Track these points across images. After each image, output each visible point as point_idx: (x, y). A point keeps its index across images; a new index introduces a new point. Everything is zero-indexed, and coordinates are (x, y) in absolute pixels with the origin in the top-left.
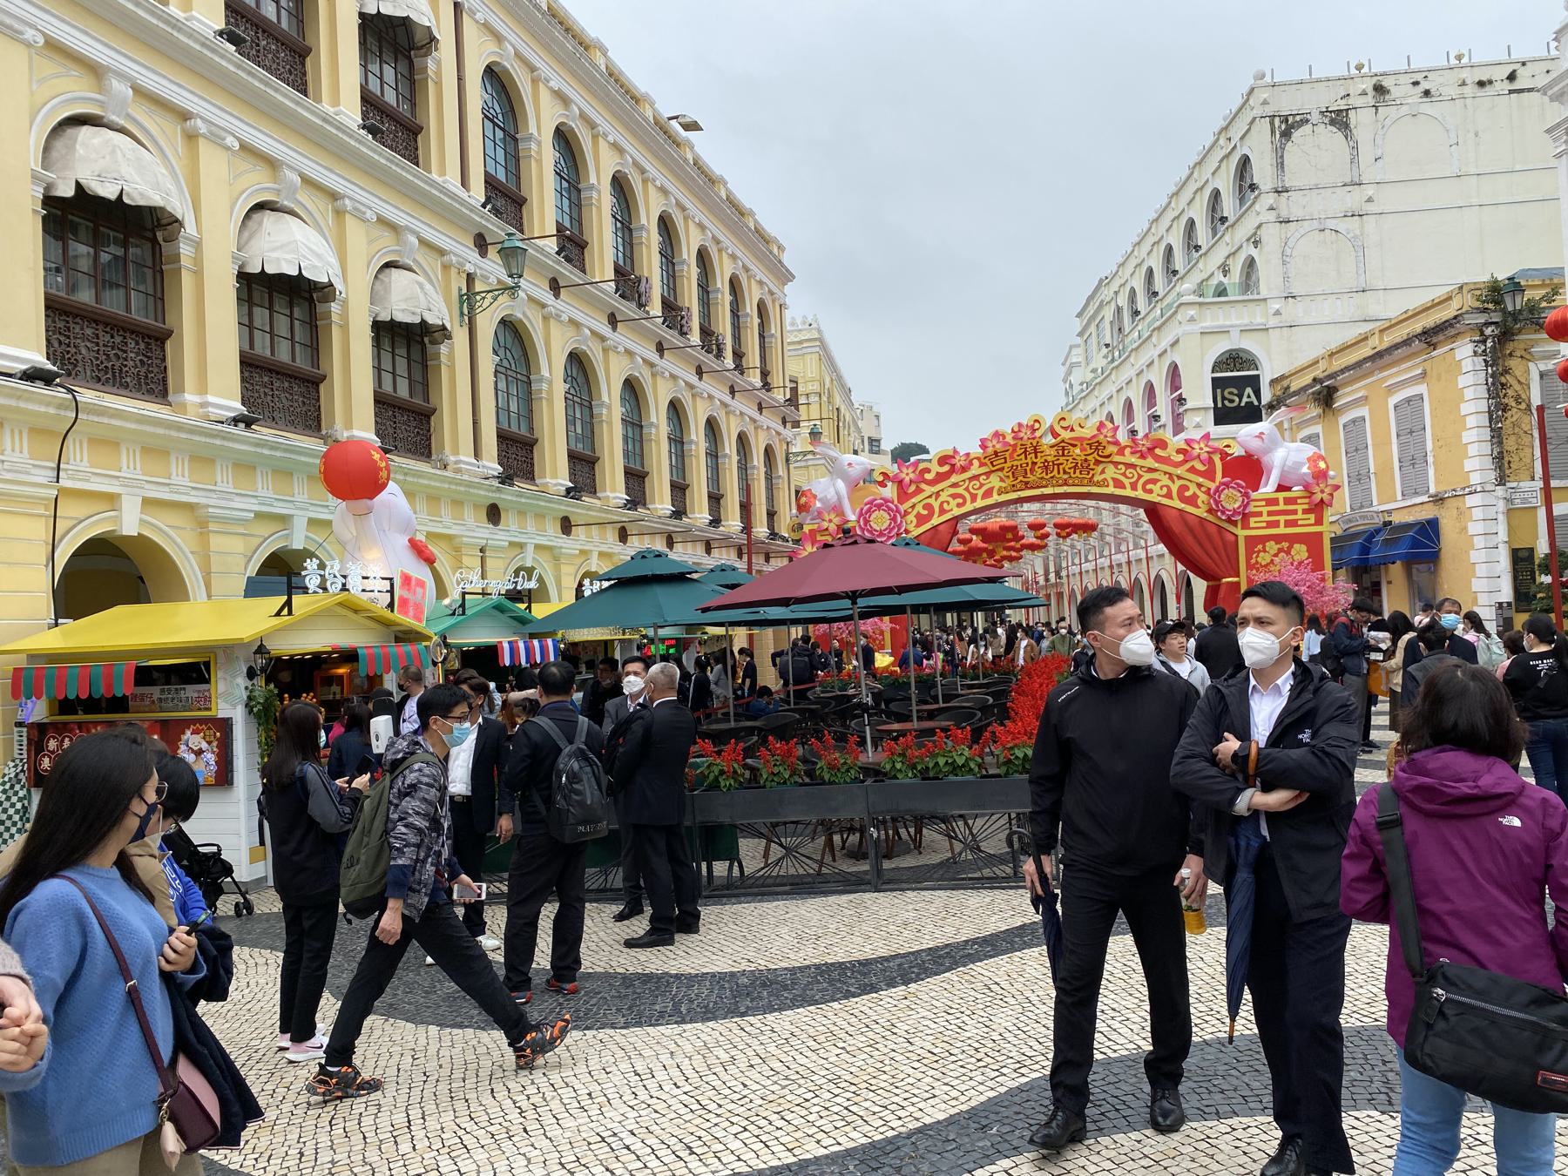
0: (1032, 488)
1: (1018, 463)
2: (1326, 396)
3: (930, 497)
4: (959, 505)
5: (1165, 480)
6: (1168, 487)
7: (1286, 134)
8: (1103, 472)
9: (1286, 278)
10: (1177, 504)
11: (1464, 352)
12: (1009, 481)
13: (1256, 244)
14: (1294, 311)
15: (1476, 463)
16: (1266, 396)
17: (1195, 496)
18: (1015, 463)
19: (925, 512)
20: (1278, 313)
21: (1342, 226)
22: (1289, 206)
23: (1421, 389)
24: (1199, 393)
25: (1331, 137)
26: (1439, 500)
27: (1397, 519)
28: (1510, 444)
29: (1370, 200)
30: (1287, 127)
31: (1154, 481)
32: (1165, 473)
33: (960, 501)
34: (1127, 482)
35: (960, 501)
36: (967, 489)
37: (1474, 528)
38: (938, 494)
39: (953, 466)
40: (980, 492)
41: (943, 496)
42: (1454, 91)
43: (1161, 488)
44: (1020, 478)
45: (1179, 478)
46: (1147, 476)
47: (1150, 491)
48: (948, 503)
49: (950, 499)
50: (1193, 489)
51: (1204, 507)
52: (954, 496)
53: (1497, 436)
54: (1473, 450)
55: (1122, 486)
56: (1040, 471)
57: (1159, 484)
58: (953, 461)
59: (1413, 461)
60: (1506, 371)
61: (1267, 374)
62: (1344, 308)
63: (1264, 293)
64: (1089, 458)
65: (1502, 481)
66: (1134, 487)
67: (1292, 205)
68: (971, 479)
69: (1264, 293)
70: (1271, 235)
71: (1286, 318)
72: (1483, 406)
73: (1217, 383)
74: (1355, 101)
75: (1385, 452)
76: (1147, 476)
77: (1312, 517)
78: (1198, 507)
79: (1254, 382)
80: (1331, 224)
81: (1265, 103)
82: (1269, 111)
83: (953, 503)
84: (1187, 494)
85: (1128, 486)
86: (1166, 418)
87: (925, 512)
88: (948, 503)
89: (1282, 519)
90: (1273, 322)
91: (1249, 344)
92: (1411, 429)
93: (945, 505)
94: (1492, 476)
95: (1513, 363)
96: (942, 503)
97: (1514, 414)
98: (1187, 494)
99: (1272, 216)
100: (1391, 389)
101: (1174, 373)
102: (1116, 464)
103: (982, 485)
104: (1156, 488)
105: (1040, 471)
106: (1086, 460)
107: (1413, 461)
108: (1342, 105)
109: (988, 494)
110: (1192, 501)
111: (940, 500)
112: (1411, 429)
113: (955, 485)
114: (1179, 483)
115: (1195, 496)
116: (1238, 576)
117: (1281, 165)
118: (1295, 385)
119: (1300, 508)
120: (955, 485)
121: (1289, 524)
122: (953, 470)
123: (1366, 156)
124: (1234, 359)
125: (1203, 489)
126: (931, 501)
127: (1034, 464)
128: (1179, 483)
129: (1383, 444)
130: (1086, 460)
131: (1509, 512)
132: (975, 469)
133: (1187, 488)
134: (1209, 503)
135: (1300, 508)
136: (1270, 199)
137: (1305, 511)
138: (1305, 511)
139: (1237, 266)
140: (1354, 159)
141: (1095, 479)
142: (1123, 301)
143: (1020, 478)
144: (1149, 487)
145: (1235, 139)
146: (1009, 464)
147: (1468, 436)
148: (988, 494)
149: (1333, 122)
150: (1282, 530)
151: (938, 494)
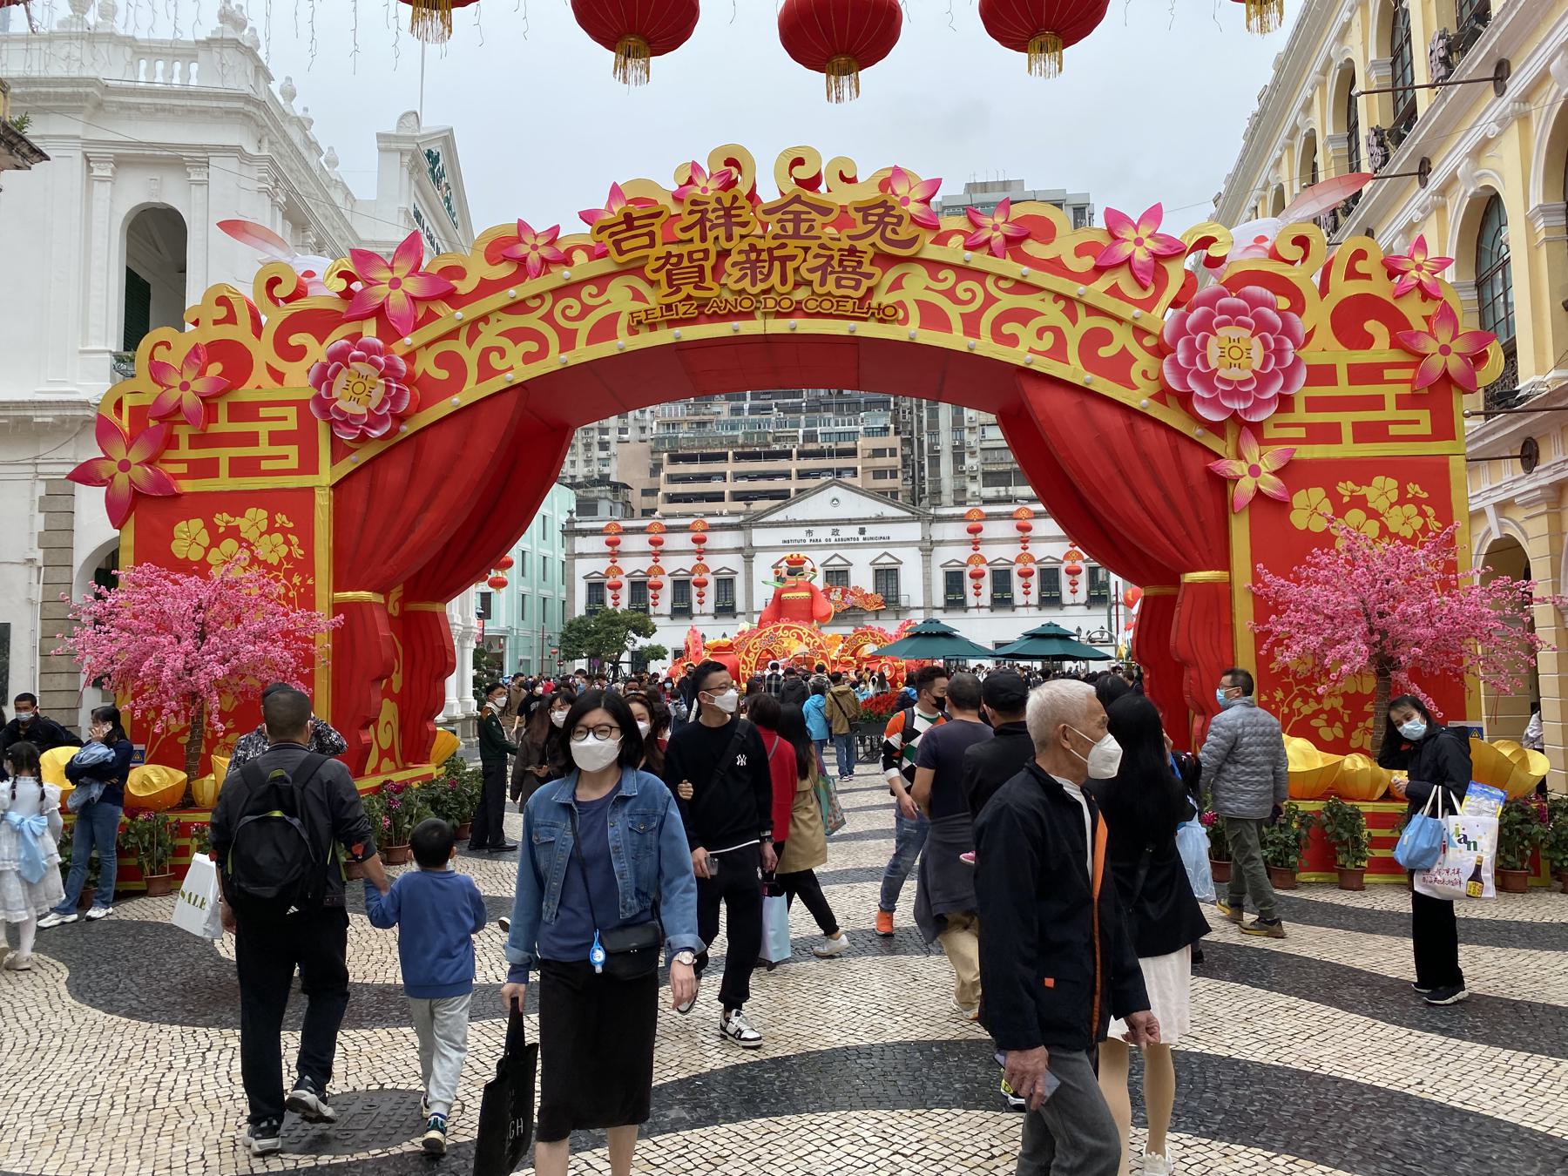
0: (715, 317)
1: (684, 249)
3: (453, 334)
4: (528, 358)
5: (1053, 314)
6: (1057, 332)
8: (897, 285)
10: (1073, 370)
12: (654, 298)
17: (1125, 358)
18: (675, 249)
19: (443, 375)
31: (1024, 316)
32: (1058, 296)
33: (533, 346)
34: (954, 312)
35: (533, 346)
36: (548, 318)
38: (473, 329)
39: (522, 261)
40: (584, 328)
41: (489, 336)
43: (1040, 333)
44: (688, 289)
45: (1092, 310)
46: (1008, 302)
47: (1012, 340)
48: (502, 353)
49: (505, 343)
50: (1122, 338)
51: (1151, 387)
52: (517, 335)
55: (946, 326)
56: (737, 274)
57: (1036, 323)
58: (523, 250)
64: (861, 245)
66: (971, 325)
68: (559, 292)
76: (1008, 302)
77: (1424, 416)
78: (1133, 387)
83: (515, 352)
84: (1104, 352)
85: (957, 324)
87: (443, 375)
88: (502, 353)
89: (1346, 419)
93: (494, 358)
96: (485, 353)
98: (1104, 352)
102: (934, 266)
103: (586, 310)
104: (1026, 334)
105: (737, 274)
106: (852, 251)
109: (605, 329)
110: (1119, 368)
111: (481, 343)
113: (517, 307)
114: (1086, 323)
115: (1125, 358)
116: (1225, 563)
119: (1389, 392)
120: (517, 307)
121: (1364, 433)
122: (523, 270)
125: (1149, 342)
126: (459, 346)
127: (724, 254)
128: (1086, 323)
130: (852, 251)
132: (582, 266)
133: (1105, 337)
134: (1160, 378)
135: (1389, 392)
137: (1403, 402)
138: (1403, 402)
141: (882, 298)
143: (688, 289)
144: (1008, 328)
146: (660, 250)
148: (605, 329)
150: (1347, 449)
151: (473, 329)
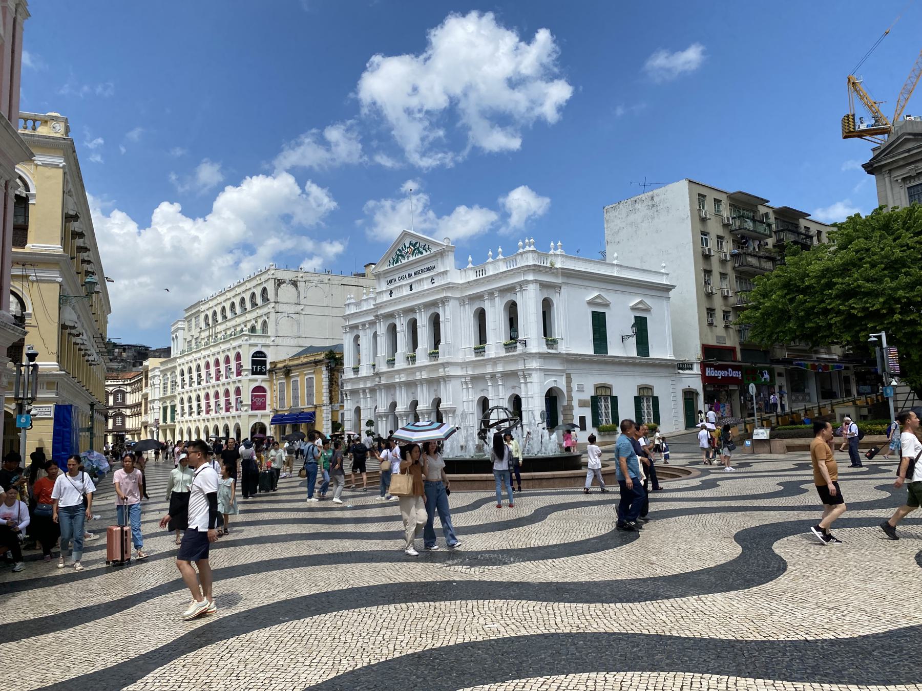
2: (287, 371)
7: (279, 285)
9: (277, 330)
11: (324, 368)
13: (268, 318)
14: (279, 341)
15: (325, 398)
16: (268, 367)
20: (273, 341)
21: (294, 316)
22: (280, 308)
23: (314, 376)
24: (247, 364)
25: (291, 288)
26: (316, 407)
27: (305, 411)
28: (333, 393)
29: (302, 310)
30: (279, 283)
37: (324, 415)
42: (327, 281)
53: (330, 392)
54: (325, 394)
59: (310, 395)
60: (334, 375)
61: (269, 360)
62: (293, 342)
63: (269, 334)
65: (331, 403)
67: (280, 308)
69: (269, 334)
70: (272, 316)
71: (276, 343)
72: (327, 383)
73: (254, 363)
74: (299, 279)
75: (303, 391)
79: (264, 363)
80: (291, 315)
81: (273, 274)
82: (274, 277)
86: (234, 370)
90: (271, 344)
91: (263, 350)
92: (310, 386)
94: (328, 402)
95: (335, 373)
97: (334, 386)
99: (273, 310)
100: (306, 375)
101: (238, 357)
107: (310, 395)
108: (295, 279)
112: (310, 386)
117: (277, 294)
118: (279, 366)
123: (302, 297)
124: (259, 354)
129: (302, 389)
131: (332, 411)
136: (273, 305)
139: (260, 321)
140: (298, 296)
142: (210, 314)
145: (263, 280)
147: (324, 391)
149: (292, 284)
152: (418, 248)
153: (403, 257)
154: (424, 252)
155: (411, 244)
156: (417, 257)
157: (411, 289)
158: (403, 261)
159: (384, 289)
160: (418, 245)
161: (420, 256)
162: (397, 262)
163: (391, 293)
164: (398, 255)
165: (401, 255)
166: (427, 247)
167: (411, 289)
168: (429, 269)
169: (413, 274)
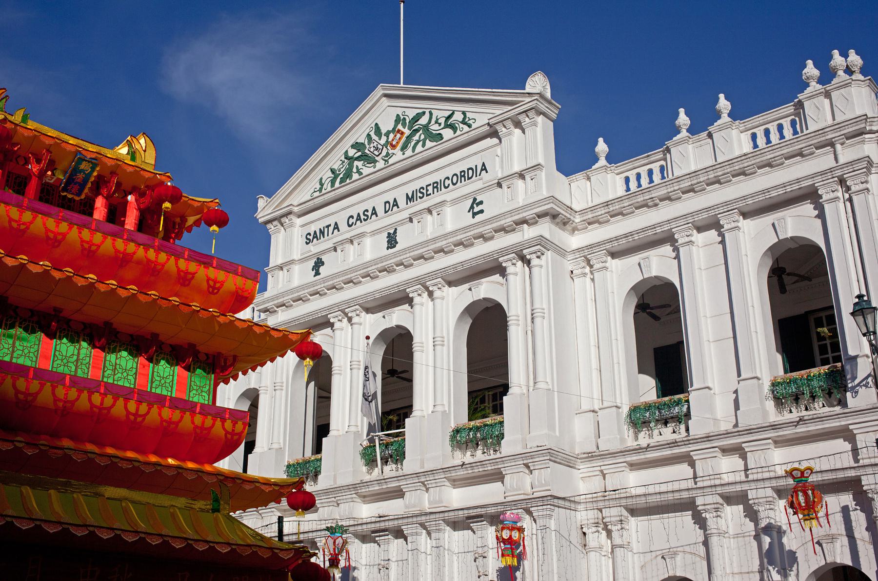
152: (426, 127)
153: (369, 160)
154: (447, 133)
155: (398, 120)
156: (419, 148)
157: (392, 241)
158: (366, 171)
159: (296, 256)
160: (424, 121)
161: (429, 144)
162: (348, 175)
163: (319, 264)
164: (351, 159)
165: (358, 159)
166: (458, 117)
167: (392, 241)
168: (463, 176)
169: (402, 202)
